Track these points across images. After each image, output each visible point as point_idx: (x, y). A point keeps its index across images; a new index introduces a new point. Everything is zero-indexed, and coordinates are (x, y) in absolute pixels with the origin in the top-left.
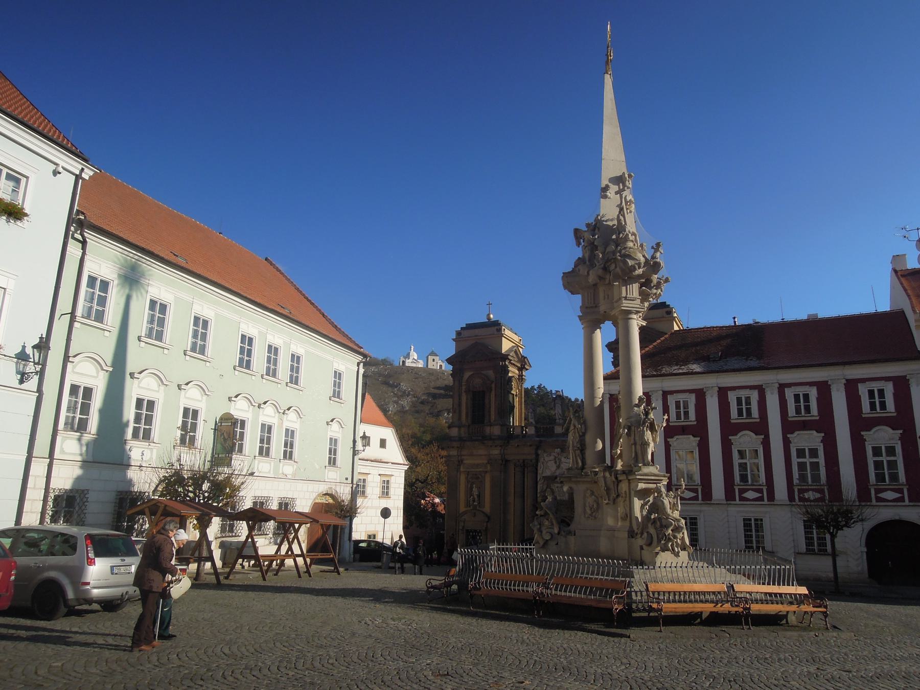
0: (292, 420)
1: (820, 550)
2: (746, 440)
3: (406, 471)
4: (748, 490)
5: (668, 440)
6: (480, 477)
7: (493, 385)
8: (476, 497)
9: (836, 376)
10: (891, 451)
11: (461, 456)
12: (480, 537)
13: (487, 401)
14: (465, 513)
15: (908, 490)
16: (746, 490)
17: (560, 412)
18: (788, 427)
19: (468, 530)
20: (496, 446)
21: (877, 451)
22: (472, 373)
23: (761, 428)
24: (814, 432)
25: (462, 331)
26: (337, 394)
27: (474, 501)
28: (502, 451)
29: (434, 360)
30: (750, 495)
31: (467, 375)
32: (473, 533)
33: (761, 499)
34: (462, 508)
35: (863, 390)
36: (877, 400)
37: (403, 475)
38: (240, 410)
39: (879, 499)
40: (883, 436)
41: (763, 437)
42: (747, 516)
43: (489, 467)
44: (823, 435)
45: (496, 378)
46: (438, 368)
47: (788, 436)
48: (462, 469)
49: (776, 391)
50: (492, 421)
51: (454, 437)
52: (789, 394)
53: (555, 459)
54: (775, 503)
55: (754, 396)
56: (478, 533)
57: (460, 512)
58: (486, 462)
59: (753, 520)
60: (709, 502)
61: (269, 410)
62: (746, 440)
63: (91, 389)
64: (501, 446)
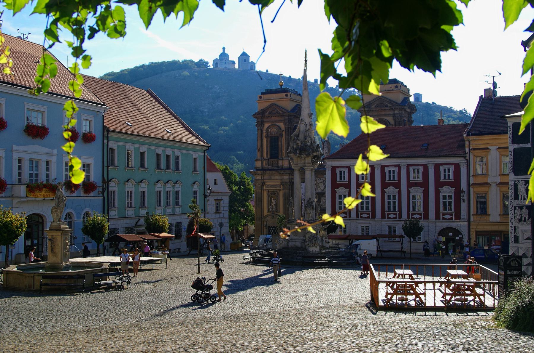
0: (178, 188)
1: (419, 240)
2: (391, 191)
3: (229, 197)
4: (391, 214)
5: (358, 190)
6: (276, 193)
7: (284, 133)
8: (274, 206)
9: (430, 162)
10: (450, 197)
11: (264, 179)
12: (277, 231)
13: (280, 143)
14: (267, 216)
15: (455, 214)
16: (390, 214)
17: (327, 151)
18: (410, 185)
19: (269, 227)
20: (286, 174)
21: (445, 197)
22: (270, 124)
23: (398, 185)
24: (420, 188)
25: (262, 95)
26: (195, 170)
27: (273, 208)
28: (290, 176)
29: (245, 61)
30: (392, 216)
31: (267, 125)
32: (272, 228)
33: (396, 218)
34: (265, 213)
35: (442, 168)
36: (447, 174)
37: (228, 198)
38: (159, 187)
39: (443, 218)
40: (447, 190)
41: (398, 189)
42: (390, 225)
43: (282, 186)
44: (423, 189)
45: (285, 128)
46: (249, 68)
47: (409, 189)
48: (264, 189)
49: (405, 168)
50: (283, 157)
51: (259, 167)
52: (411, 169)
53: (323, 182)
54: (402, 220)
55: (396, 169)
56: (276, 228)
57: (264, 215)
58: (279, 183)
59: (392, 227)
60: (374, 219)
61: (169, 185)
62: (391, 191)
63: (114, 191)
64: (289, 174)
